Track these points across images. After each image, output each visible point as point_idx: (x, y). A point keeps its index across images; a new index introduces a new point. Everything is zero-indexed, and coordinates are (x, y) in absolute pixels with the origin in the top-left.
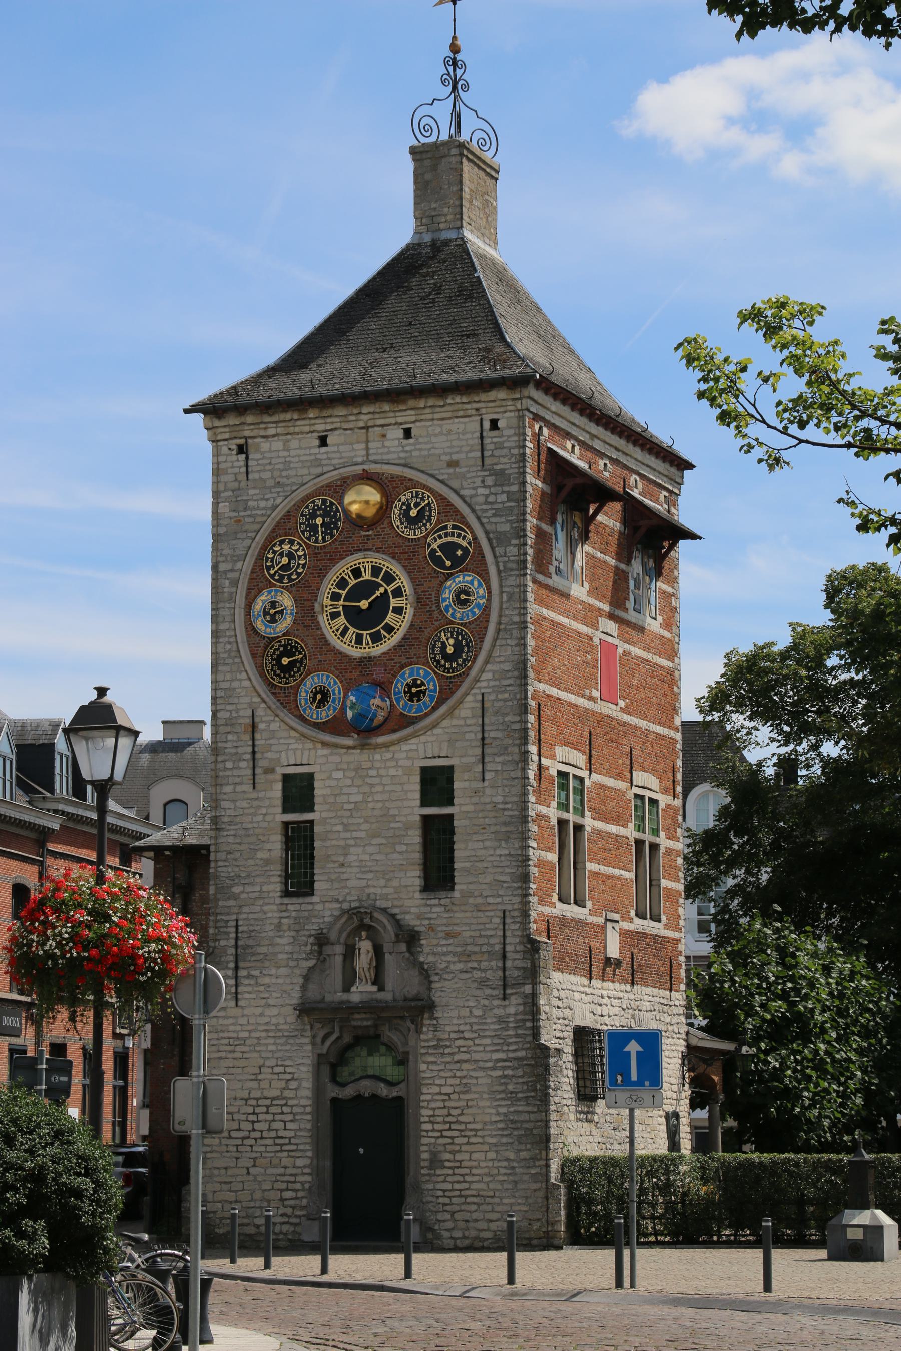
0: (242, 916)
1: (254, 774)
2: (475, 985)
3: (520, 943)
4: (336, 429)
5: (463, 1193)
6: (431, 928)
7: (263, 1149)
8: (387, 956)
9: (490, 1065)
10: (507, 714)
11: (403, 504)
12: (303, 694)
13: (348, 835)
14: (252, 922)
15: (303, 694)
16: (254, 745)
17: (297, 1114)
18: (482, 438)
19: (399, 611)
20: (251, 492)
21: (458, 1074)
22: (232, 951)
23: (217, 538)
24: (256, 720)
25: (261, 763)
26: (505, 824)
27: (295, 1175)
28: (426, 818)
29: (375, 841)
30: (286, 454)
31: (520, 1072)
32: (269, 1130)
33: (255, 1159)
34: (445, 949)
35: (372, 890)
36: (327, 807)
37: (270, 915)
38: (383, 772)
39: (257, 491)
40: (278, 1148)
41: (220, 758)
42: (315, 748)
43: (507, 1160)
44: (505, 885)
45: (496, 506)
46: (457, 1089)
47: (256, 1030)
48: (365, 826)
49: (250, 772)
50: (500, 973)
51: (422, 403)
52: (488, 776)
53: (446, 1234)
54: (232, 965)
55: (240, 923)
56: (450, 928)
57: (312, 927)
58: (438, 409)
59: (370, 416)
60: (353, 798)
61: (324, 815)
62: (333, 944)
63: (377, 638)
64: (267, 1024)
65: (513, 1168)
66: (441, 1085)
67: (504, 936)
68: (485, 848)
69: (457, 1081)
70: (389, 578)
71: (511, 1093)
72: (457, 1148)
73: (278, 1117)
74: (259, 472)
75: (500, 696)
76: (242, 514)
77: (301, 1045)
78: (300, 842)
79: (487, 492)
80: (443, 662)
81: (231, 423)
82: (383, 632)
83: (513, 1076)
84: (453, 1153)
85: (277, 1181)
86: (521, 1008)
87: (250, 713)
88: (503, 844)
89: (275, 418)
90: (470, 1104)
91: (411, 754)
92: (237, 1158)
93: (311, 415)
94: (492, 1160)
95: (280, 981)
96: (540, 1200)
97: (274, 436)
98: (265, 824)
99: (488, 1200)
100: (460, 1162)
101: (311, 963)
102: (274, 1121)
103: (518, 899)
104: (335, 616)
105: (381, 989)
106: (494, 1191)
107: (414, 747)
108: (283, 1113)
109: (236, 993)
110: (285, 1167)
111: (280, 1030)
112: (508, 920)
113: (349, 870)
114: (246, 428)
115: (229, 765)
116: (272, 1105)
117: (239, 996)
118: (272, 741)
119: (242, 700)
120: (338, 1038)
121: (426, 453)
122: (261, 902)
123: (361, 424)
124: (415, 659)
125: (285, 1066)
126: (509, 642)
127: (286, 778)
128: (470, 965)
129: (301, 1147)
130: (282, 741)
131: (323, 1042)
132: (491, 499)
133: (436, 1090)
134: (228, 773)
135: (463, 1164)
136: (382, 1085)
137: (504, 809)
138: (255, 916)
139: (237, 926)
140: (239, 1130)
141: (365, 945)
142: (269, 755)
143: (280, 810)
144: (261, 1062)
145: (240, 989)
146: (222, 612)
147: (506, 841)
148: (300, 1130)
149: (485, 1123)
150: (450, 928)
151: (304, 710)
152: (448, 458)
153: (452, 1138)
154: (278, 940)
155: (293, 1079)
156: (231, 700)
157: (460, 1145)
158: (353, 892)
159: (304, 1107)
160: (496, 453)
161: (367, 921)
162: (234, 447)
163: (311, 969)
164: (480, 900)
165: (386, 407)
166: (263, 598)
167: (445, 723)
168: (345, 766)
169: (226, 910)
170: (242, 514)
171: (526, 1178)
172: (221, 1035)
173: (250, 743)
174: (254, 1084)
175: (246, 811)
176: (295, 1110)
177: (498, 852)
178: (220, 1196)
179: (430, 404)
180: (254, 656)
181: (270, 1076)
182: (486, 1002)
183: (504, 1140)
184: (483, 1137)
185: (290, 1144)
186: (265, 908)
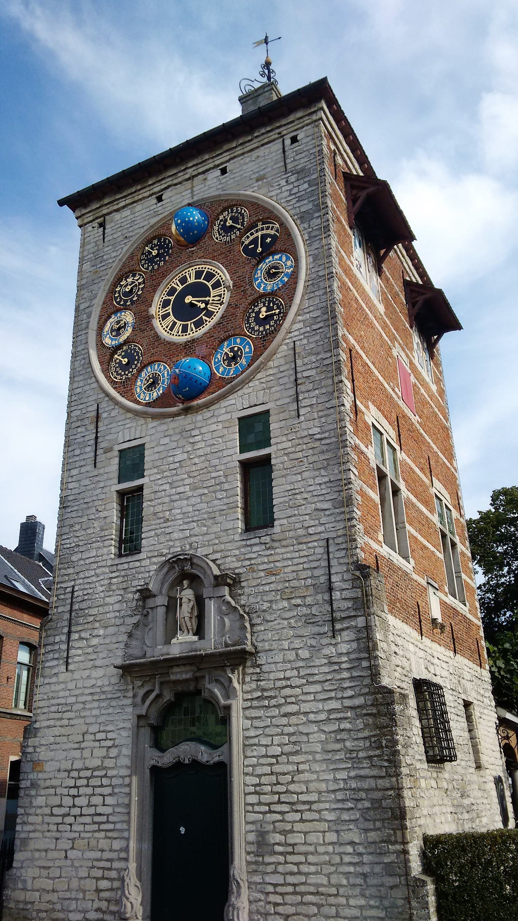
0: (78, 582)
2: (300, 624)
3: (348, 571)
4: (169, 187)
5: (298, 889)
6: (252, 569)
7: (81, 828)
9: (323, 716)
10: (318, 354)
11: (221, 221)
14: (87, 586)
16: (97, 432)
18: (284, 152)
21: (287, 730)
22: (67, 616)
23: (80, 288)
25: (102, 445)
26: (323, 452)
34: (267, 588)
36: (155, 471)
38: (203, 430)
39: (110, 247)
41: (70, 449)
42: (146, 423)
43: (352, 843)
44: (327, 513)
46: (287, 749)
47: (82, 694)
48: (190, 481)
49: (93, 454)
52: (302, 411)
54: (66, 630)
55: (76, 588)
57: (139, 583)
58: (247, 144)
62: (155, 596)
63: (199, 324)
65: (360, 854)
67: (329, 566)
70: (210, 276)
72: (288, 827)
73: (98, 790)
75: (311, 340)
80: (257, 328)
81: (94, 208)
82: (204, 317)
83: (350, 730)
85: (93, 867)
86: (355, 645)
88: (323, 472)
91: (229, 409)
92: (57, 839)
93: (150, 182)
95: (107, 641)
96: (400, 902)
97: (124, 207)
99: (332, 900)
100: (293, 845)
101: (135, 620)
102: (93, 795)
103: (341, 525)
104: (165, 317)
106: (338, 886)
107: (233, 402)
108: (102, 786)
110: (102, 851)
111: (104, 692)
114: (104, 208)
115: (77, 452)
116: (92, 777)
117: (70, 661)
119: (91, 399)
120: (158, 696)
121: (239, 178)
122: (95, 566)
123: (187, 176)
124: (231, 332)
126: (317, 293)
128: (293, 601)
129: (118, 826)
130: (119, 424)
131: (143, 701)
132: (295, 190)
135: (297, 849)
136: (203, 748)
140: (60, 806)
141: (187, 594)
144: (84, 728)
146: (80, 338)
147: (324, 468)
148: (118, 805)
149: (320, 793)
151: (139, 396)
152: (257, 175)
155: (114, 746)
161: (188, 567)
163: (136, 625)
164: (301, 532)
166: (111, 320)
167: (259, 376)
168: (171, 432)
171: (378, 869)
173: (95, 431)
174: (77, 754)
175: (88, 488)
176: (115, 781)
177: (318, 480)
178: (38, 884)
179: (239, 143)
181: (92, 744)
182: (313, 642)
183: (345, 816)
184: (319, 811)
185: (108, 822)
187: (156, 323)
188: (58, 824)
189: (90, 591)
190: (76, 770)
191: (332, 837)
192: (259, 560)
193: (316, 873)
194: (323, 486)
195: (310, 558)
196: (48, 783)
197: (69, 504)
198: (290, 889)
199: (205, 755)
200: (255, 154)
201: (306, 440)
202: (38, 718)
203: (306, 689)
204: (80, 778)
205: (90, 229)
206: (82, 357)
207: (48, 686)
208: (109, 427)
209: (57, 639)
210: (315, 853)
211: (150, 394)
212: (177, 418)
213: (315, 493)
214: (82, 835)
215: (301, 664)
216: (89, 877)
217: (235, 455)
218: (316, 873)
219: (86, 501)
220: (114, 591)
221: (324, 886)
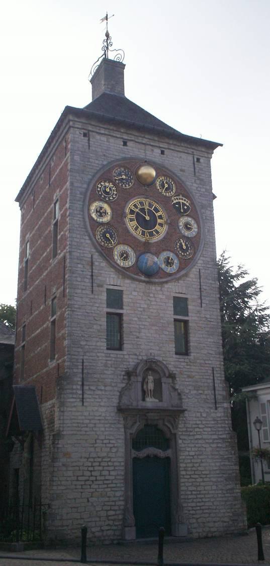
1: (92, 286)
6: (181, 373)
7: (96, 487)
8: (163, 384)
9: (211, 441)
12: (116, 253)
13: (141, 323)
14: (91, 361)
15: (116, 253)
16: (92, 272)
17: (116, 466)
18: (194, 164)
19: (161, 225)
20: (91, 155)
24: (94, 260)
25: (96, 281)
27: (115, 501)
28: (175, 320)
29: (154, 328)
30: (108, 144)
31: (224, 445)
32: (101, 475)
33: (92, 493)
34: (188, 383)
35: (153, 351)
37: (100, 358)
40: (106, 486)
45: (201, 192)
46: (197, 453)
48: (149, 320)
49: (90, 285)
50: (213, 397)
51: (171, 142)
52: (203, 305)
53: (194, 531)
54: (80, 383)
55: (85, 361)
56: (189, 373)
59: (148, 140)
60: (142, 306)
61: (128, 312)
63: (151, 234)
64: (100, 416)
65: (224, 494)
66: (189, 451)
68: (203, 338)
69: (196, 449)
71: (221, 455)
72: (198, 484)
73: (105, 468)
74: (95, 147)
76: (86, 163)
77: (118, 428)
78: (116, 321)
79: (197, 186)
84: (197, 486)
87: (90, 256)
89: (105, 126)
90: (203, 461)
92: (82, 493)
93: (122, 131)
94: (215, 490)
95: (107, 393)
97: (102, 134)
98: (98, 312)
99: (214, 511)
100: (200, 491)
101: (124, 385)
102: (103, 470)
105: (161, 401)
107: (170, 287)
108: (108, 466)
109: (83, 398)
110: (109, 497)
112: (215, 372)
113: (141, 340)
115: (79, 279)
116: (102, 461)
117: (84, 400)
118: (101, 272)
123: (144, 142)
125: (109, 440)
127: (109, 291)
129: (118, 485)
132: (199, 189)
133: (187, 453)
134: (78, 283)
137: (210, 321)
138: (93, 358)
139: (83, 362)
140: (83, 476)
141: (151, 378)
142: (100, 278)
143: (105, 306)
145: (85, 396)
148: (118, 475)
149: (210, 471)
150: (189, 373)
151: (117, 261)
153: (195, 478)
154: (105, 372)
156: (80, 248)
157: (200, 482)
158: (144, 351)
159: (120, 462)
160: (200, 172)
162: (82, 133)
164: (202, 361)
165: (156, 139)
169: (76, 353)
170: (86, 163)
172: (73, 421)
173: (90, 270)
174: (92, 449)
175: (88, 304)
177: (209, 340)
180: (92, 229)
183: (219, 480)
184: (210, 478)
185: (112, 483)
186: (98, 354)
187: (127, 220)
188: (82, 485)
189: (95, 364)
190: (92, 458)
191: (214, 487)
192: (184, 370)
193: (208, 501)
194: (211, 343)
195: (206, 374)
196: (75, 464)
197: (75, 310)
198: (199, 508)
199: (161, 453)
200: (180, 154)
201: (204, 319)
202: (64, 429)
203: (205, 429)
204: (95, 462)
205: (78, 132)
206: (77, 218)
207: (70, 413)
208: (99, 272)
209: (74, 387)
210: (208, 494)
211: (123, 263)
212: (141, 283)
213: (208, 345)
214: (98, 490)
215: (203, 419)
216: (102, 510)
217: (169, 315)
218: (208, 501)
219: (87, 311)
220: (109, 367)
221: (211, 506)
